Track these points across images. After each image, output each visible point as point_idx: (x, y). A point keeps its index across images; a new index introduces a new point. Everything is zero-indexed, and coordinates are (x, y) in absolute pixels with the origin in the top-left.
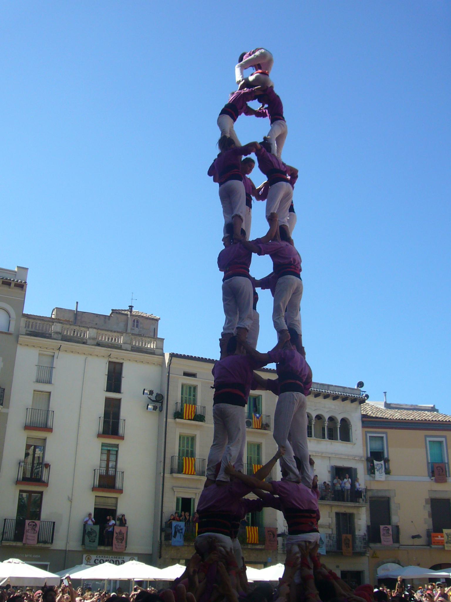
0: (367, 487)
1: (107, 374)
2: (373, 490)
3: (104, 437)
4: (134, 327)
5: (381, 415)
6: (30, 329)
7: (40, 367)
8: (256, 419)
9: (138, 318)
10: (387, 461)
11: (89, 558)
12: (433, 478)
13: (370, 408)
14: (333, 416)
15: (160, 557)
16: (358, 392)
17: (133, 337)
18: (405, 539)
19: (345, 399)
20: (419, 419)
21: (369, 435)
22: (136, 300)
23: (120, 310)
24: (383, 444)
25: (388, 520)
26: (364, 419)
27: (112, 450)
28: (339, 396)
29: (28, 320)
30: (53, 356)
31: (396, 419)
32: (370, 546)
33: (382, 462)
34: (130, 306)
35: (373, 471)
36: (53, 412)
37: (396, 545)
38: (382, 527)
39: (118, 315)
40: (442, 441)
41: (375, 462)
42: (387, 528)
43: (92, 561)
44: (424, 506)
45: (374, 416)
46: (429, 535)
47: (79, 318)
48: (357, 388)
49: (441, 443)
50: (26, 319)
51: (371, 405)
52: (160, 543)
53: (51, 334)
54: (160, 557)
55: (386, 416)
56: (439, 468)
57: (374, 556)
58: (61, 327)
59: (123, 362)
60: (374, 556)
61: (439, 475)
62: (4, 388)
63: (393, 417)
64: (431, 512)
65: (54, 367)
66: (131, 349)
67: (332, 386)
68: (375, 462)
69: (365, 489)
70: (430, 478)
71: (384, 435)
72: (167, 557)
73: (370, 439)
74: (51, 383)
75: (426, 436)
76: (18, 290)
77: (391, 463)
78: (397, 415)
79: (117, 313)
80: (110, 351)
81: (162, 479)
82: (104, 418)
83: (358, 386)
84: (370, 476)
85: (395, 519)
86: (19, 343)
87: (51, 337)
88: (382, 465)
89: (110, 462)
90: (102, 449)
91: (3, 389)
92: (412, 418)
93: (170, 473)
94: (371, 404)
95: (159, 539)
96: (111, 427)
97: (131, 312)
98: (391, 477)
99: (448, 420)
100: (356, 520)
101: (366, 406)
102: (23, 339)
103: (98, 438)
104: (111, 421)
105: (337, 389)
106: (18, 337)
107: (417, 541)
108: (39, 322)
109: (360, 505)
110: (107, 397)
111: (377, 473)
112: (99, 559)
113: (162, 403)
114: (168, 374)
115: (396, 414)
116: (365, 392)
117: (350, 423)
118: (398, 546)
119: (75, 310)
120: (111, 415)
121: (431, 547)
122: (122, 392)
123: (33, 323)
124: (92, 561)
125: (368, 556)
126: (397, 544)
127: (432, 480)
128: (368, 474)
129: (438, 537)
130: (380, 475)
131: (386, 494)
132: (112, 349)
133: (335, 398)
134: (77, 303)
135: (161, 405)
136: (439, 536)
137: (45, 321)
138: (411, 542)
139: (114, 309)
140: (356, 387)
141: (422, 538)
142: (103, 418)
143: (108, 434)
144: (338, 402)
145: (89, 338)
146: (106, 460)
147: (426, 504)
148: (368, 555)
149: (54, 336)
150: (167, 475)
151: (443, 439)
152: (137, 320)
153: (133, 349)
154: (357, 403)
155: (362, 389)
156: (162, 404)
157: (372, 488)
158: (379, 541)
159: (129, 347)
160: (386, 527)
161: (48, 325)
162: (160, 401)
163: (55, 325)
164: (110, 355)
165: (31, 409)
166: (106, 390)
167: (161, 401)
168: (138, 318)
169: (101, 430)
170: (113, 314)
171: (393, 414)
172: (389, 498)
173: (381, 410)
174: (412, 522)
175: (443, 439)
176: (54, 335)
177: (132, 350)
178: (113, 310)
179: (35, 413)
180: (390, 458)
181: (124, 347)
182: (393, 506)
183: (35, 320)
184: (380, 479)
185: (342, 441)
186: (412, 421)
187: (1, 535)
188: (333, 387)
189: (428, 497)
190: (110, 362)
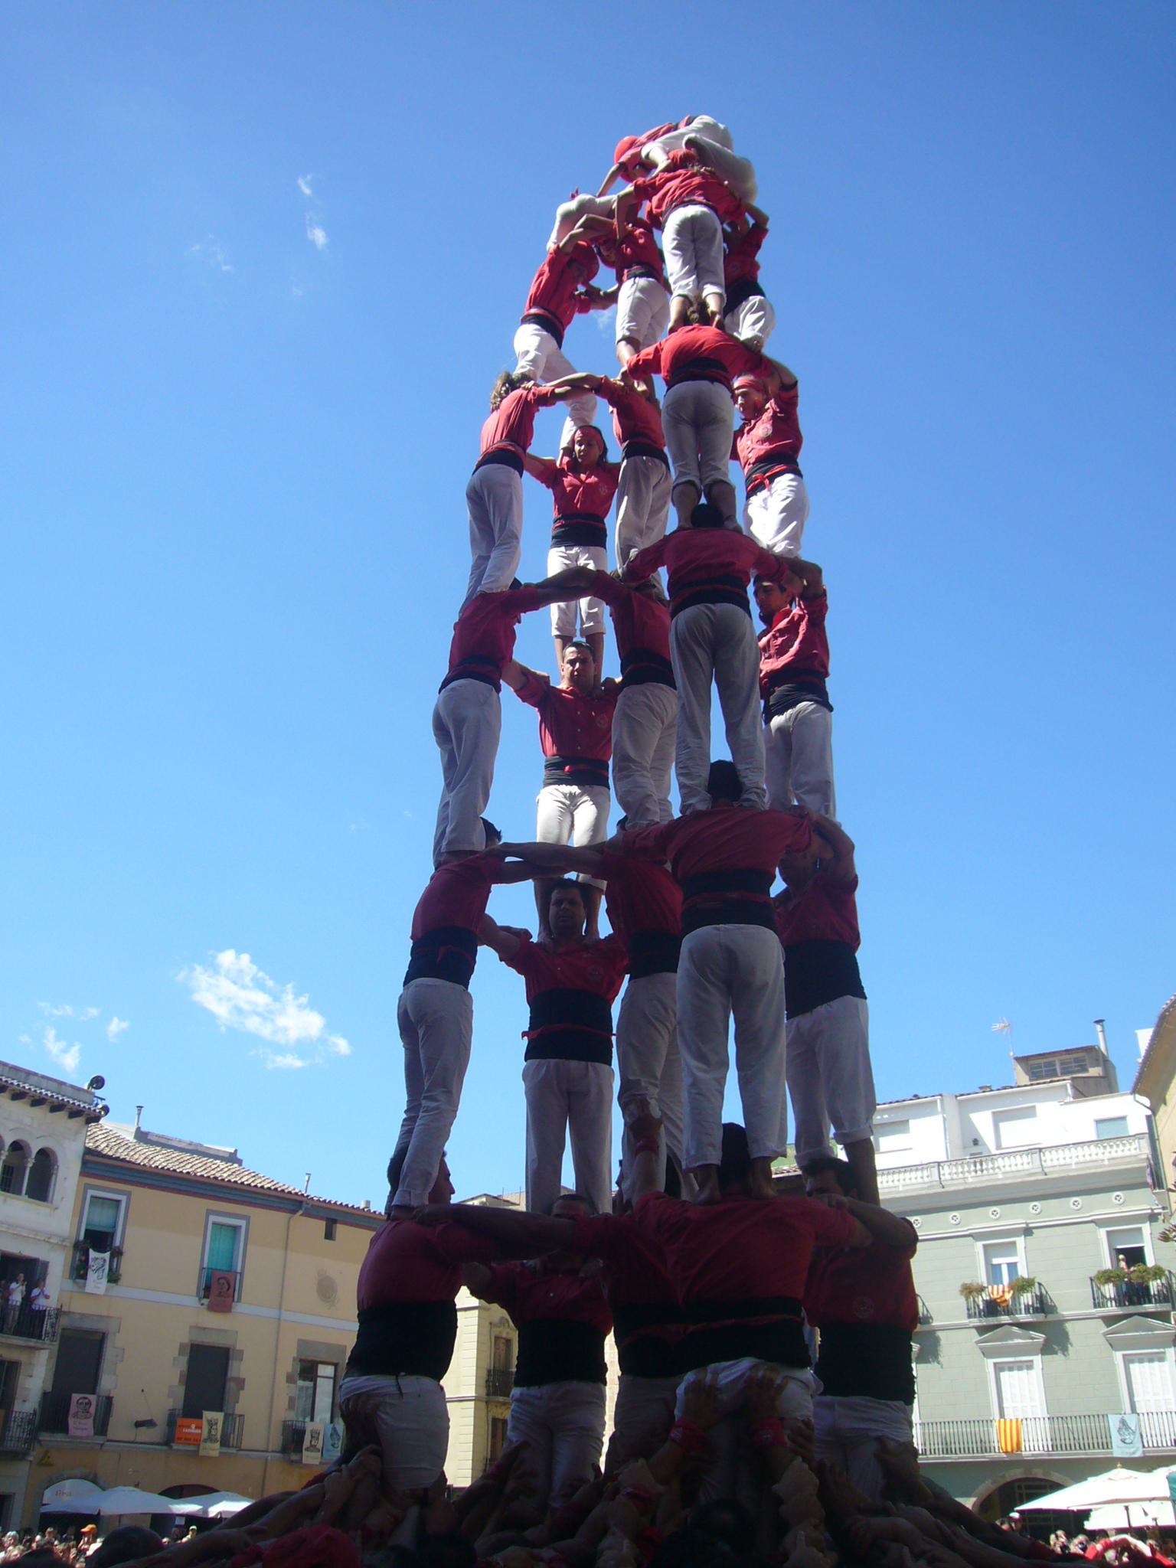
0: (62, 1306)
2: (73, 1313)
5: (126, 1153)
10: (117, 1253)
12: (206, 1301)
13: (103, 1136)
14: (22, 1141)
16: (87, 1097)
18: (120, 1427)
19: (57, 1107)
20: (202, 1173)
21: (91, 1192)
24: (116, 1217)
25: (92, 1385)
26: (88, 1157)
28: (46, 1100)
31: (157, 1167)
32: (41, 1438)
33: (107, 1255)
35: (82, 1272)
37: (100, 1439)
38: (75, 1397)
40: (240, 1227)
41: (92, 1254)
42: (87, 1401)
44: (175, 1359)
45: (110, 1153)
46: (172, 1421)
48: (88, 1088)
49: (236, 1229)
51: (106, 1129)
55: (136, 1157)
56: (222, 1281)
57: (44, 1462)
60: (44, 1462)
61: (220, 1294)
63: (151, 1163)
64: (186, 1373)
67: (36, 1074)
68: (92, 1254)
69: (58, 1309)
70: (200, 1299)
71: (123, 1198)
73: (91, 1202)
75: (209, 1212)
77: (125, 1259)
78: (160, 1159)
83: (91, 1085)
84: (74, 1282)
85: (107, 1382)
92: (189, 1170)
94: (106, 1127)
98: (118, 1290)
99: (259, 1185)
100: (21, 1378)
101: (95, 1130)
105: (44, 1083)
107: (145, 1434)
109: (39, 1345)
111: (91, 1275)
115: (157, 1158)
116: (104, 1099)
117: (57, 1162)
118: (102, 1442)
121: (172, 1447)
125: (31, 1461)
127: (202, 1304)
128: (69, 1278)
129: (189, 1427)
130: (97, 1282)
131: (100, 1326)
133: (38, 1102)
136: (193, 1426)
138: (131, 1434)
140: (86, 1087)
141: (157, 1428)
144: (41, 1112)
147: (179, 1354)
148: (31, 1458)
151: (242, 1223)
154: (81, 1120)
155: (98, 1093)
157: (71, 1310)
158: (64, 1429)
160: (86, 1398)
171: (151, 1156)
172: (104, 1334)
173: (126, 1144)
174: (143, 1391)
175: (242, 1223)
180: (125, 1249)
182: (109, 1353)
184: (94, 1291)
185: (29, 1197)
186: (187, 1176)
188: (36, 1078)
189: (186, 1340)
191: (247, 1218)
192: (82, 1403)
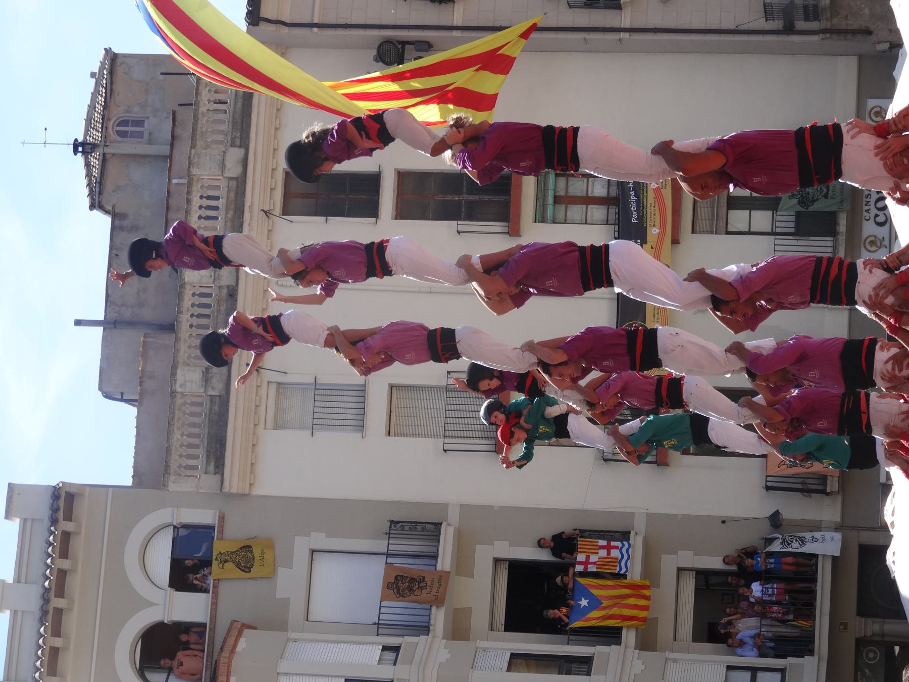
1: (323, 219)
3: (518, 216)
4: (142, 132)
6: (200, 463)
7: (316, 421)
9: (112, 121)
11: (872, 243)
15: (868, 32)
17: (199, 143)
22: (46, 129)
23: (89, 185)
27: (555, 191)
29: (172, 470)
30: (279, 384)
34: (76, 151)
36: (449, 373)
39: (109, 186)
43: (882, 232)
47: (127, 314)
50: (172, 478)
52: (828, 35)
53: (211, 396)
54: (868, 32)
58: (187, 368)
59: (282, 170)
62: (389, 523)
65: (313, 381)
66: (240, 147)
72: (867, 11)
74: (364, 385)
76: (82, 509)
79: (100, 193)
80: (251, 212)
81: (637, 37)
82: (460, 220)
86: (247, 492)
87: (220, 396)
89: (590, 194)
90: (554, 222)
91: (390, 527)
93: (618, 11)
95: (815, 38)
96: (486, 198)
97: (94, 146)
102: (233, 481)
103: (520, 236)
104: (466, 197)
106: (231, 496)
108: (177, 436)
110: (394, 217)
112: (874, 211)
113: (404, 43)
114: (315, 30)
119: (101, 329)
120: (449, 197)
122: (378, 170)
123: (181, 456)
124: (882, 232)
132: (247, 209)
134: (78, 323)
135: (412, 46)
137: (173, 418)
139: (87, 202)
142: (460, 222)
143: (506, 206)
145: (268, 290)
146: (584, 207)
149: (216, 388)
150: (626, 19)
152: (118, 125)
153: (238, 142)
156: (409, 43)
159: (235, 154)
161: (183, 408)
162: (398, 49)
163: (181, 386)
164: (265, 212)
165: (447, 440)
166: (374, 220)
167: (400, 46)
168: (112, 121)
169: (497, 226)
170: (105, 206)
176: (213, 388)
177: (244, 143)
178: (92, 207)
179: (457, 427)
181: (233, 170)
183: (173, 448)
187: (811, 497)
190: (285, 212)
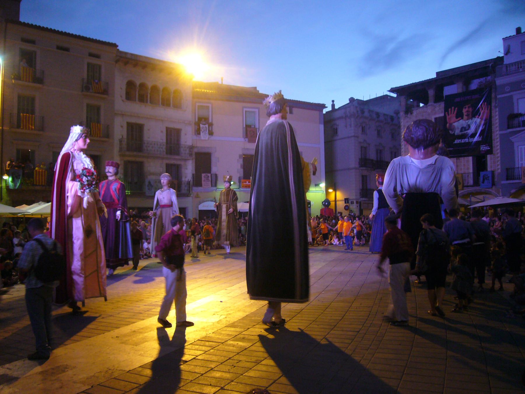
0: (192, 144)
8: (95, 85)
10: (211, 125)
38: (203, 175)
44: (238, 160)
57: (197, 197)
70: (244, 139)
85: (214, 170)
88: (206, 127)
98: (213, 138)
125: (192, 197)
126: (215, 187)
129: (246, 182)
130: (204, 136)
136: (247, 182)
148: (192, 196)
151: (257, 110)
174: (228, 171)
180: (214, 122)
182: (213, 159)
189: (241, 153)
191: (259, 108)
192: (206, 177)
